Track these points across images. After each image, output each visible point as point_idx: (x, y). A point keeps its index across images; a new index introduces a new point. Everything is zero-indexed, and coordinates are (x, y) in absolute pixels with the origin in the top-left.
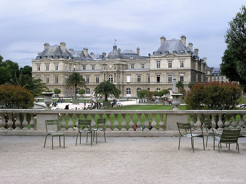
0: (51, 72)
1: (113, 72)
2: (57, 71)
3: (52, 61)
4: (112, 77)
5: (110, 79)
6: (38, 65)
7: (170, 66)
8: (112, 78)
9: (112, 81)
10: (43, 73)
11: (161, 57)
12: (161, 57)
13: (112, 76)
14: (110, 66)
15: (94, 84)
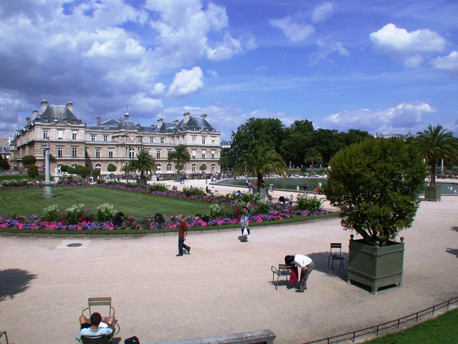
0: (68, 142)
1: (136, 145)
2: (74, 141)
3: (69, 126)
4: (133, 151)
5: (130, 153)
6: (45, 131)
7: (204, 141)
8: (133, 153)
9: (133, 155)
10: (53, 142)
11: (197, 133)
12: (197, 133)
13: (133, 150)
14: (132, 138)
15: (106, 159)
